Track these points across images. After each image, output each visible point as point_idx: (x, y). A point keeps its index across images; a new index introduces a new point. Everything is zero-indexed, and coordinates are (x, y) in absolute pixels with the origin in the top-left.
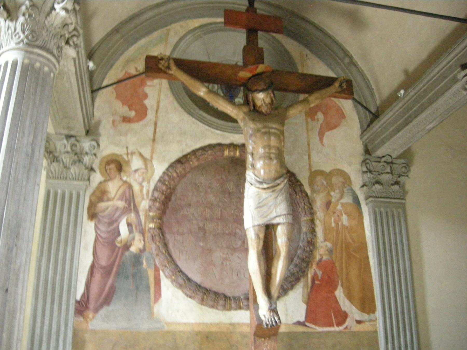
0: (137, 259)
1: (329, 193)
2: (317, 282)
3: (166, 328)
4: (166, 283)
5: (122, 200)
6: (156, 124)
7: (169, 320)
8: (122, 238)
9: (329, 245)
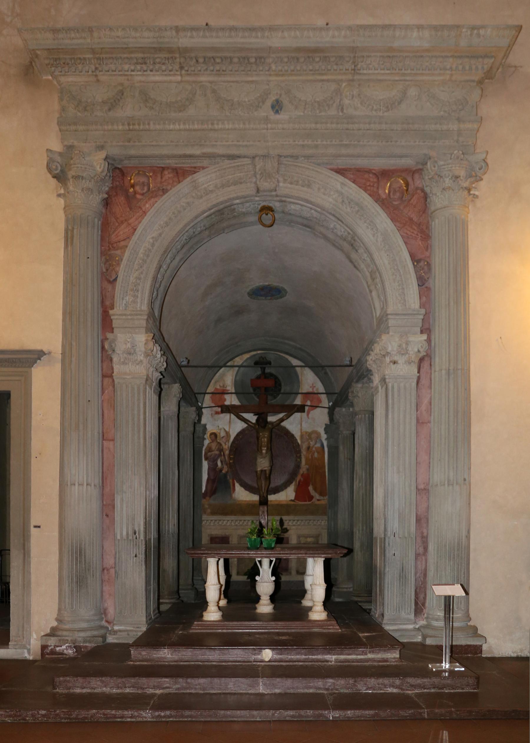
0: (225, 475)
1: (309, 443)
2: (301, 483)
3: (237, 503)
4: (237, 486)
7: (238, 500)
9: (307, 466)
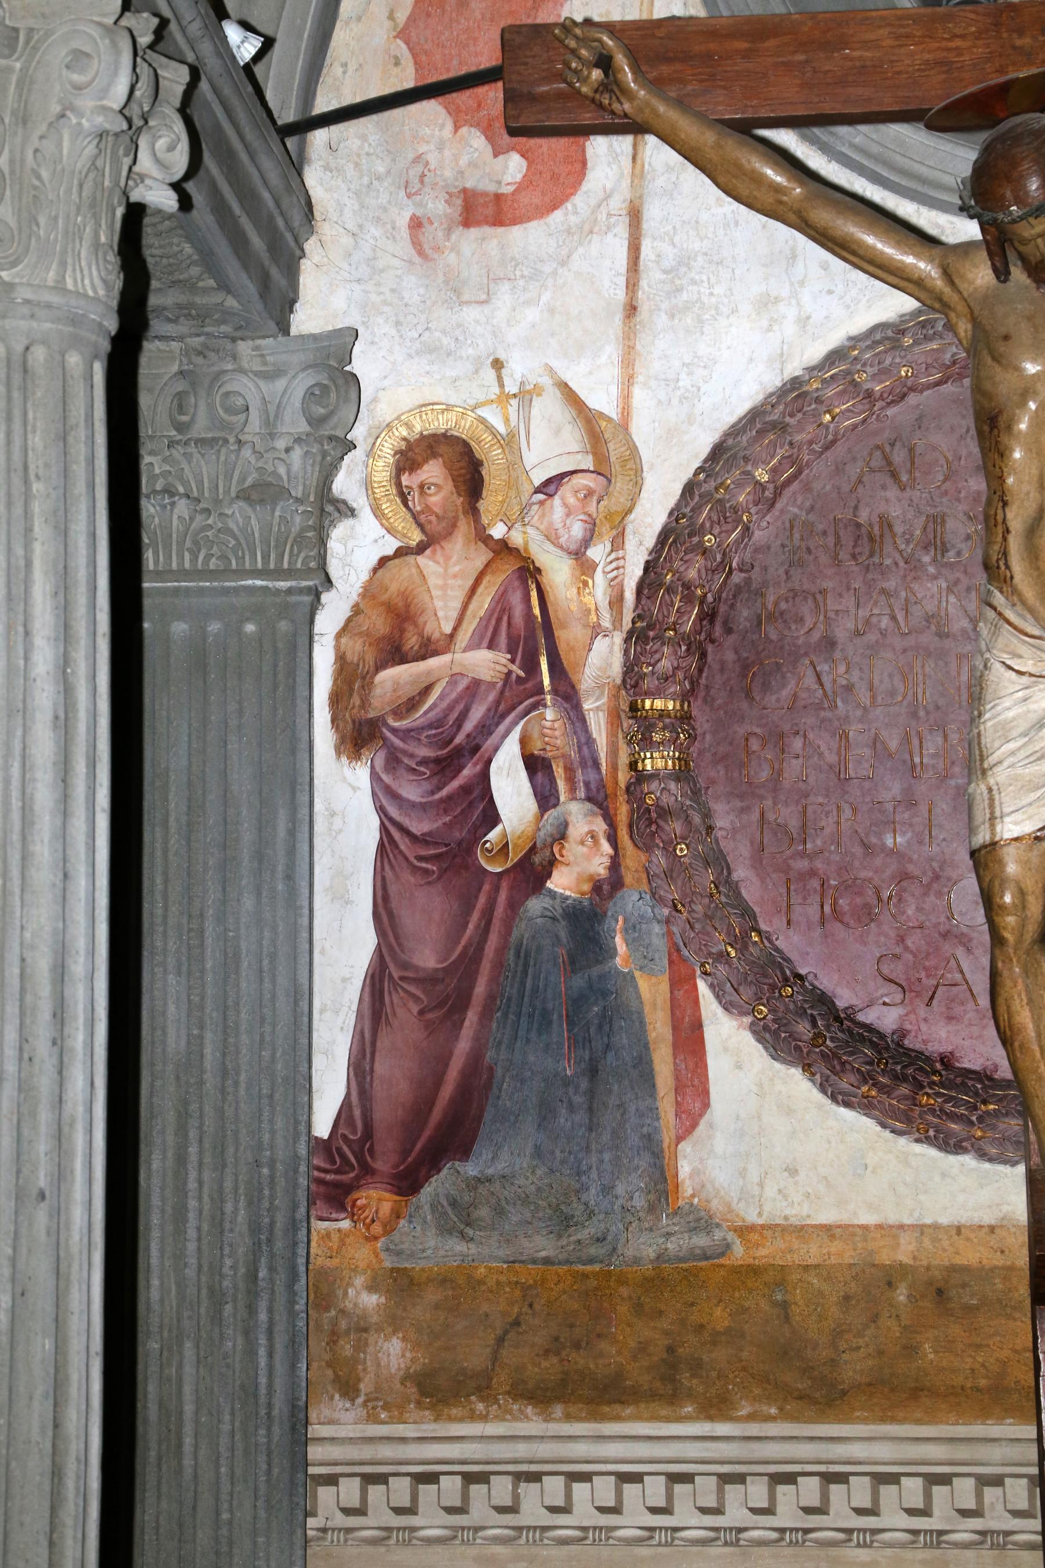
5: (490, 647)
6: (635, 216)
8: (508, 830)
